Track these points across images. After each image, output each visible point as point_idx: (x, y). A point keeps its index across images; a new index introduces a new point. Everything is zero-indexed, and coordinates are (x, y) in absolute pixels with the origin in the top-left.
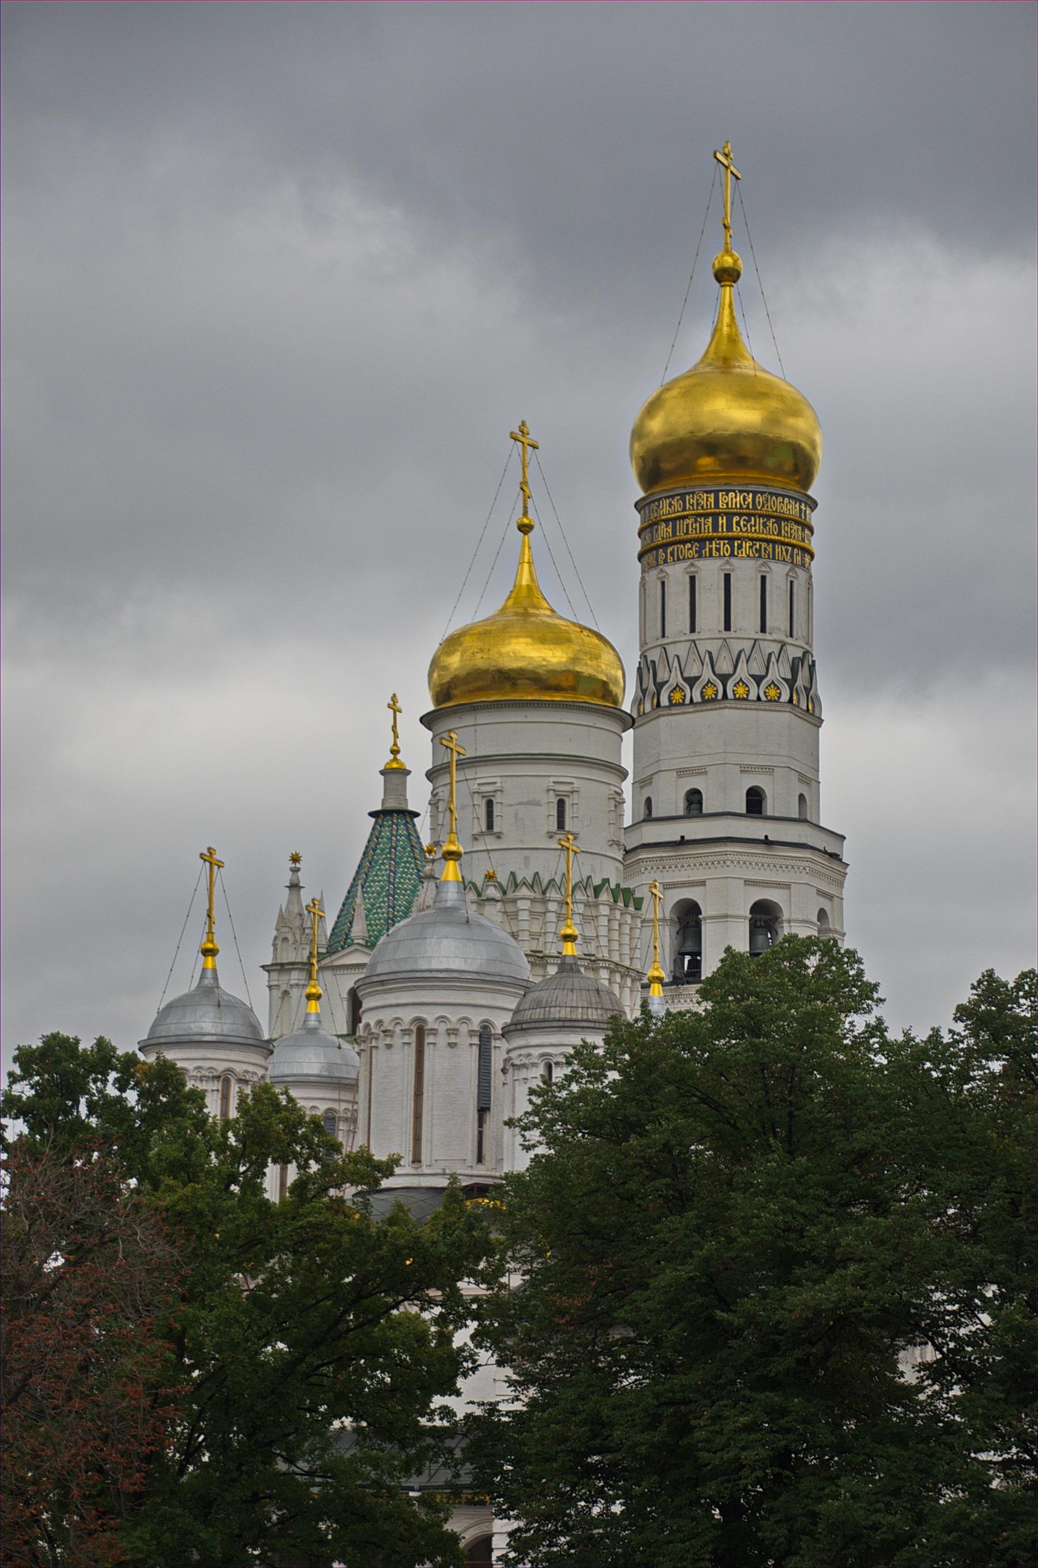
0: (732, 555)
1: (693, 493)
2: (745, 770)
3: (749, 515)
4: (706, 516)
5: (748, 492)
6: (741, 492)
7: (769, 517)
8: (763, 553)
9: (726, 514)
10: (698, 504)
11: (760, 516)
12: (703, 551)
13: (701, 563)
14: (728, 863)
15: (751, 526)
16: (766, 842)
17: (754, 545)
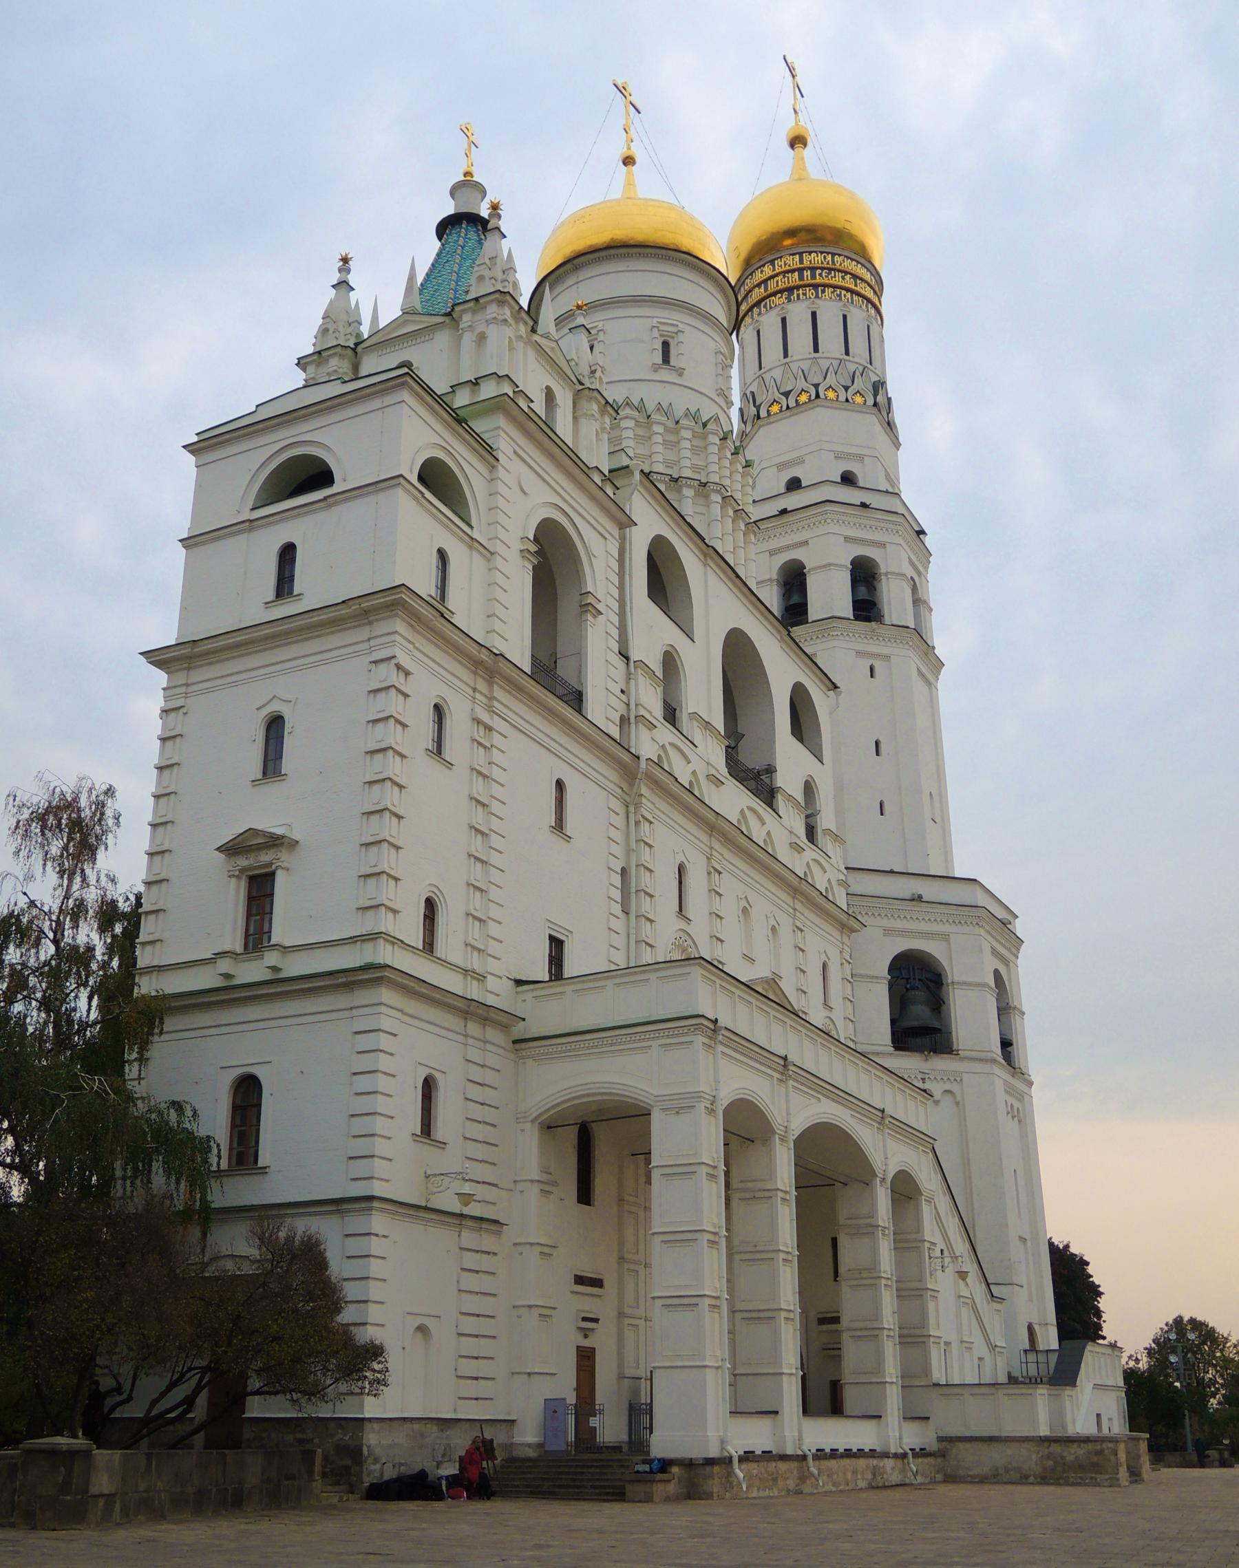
0: (817, 297)
1: (781, 257)
2: (839, 456)
3: (830, 270)
4: (792, 271)
5: (828, 253)
6: (822, 253)
7: (846, 273)
8: (843, 298)
9: (809, 268)
10: (785, 265)
11: (839, 271)
12: (792, 297)
13: (790, 306)
14: (829, 521)
15: (832, 277)
16: (864, 505)
17: (834, 291)
